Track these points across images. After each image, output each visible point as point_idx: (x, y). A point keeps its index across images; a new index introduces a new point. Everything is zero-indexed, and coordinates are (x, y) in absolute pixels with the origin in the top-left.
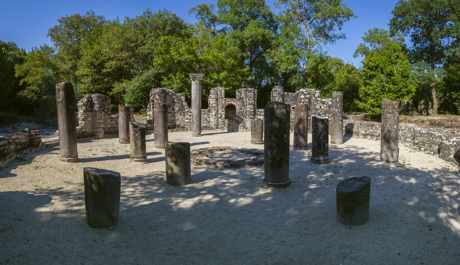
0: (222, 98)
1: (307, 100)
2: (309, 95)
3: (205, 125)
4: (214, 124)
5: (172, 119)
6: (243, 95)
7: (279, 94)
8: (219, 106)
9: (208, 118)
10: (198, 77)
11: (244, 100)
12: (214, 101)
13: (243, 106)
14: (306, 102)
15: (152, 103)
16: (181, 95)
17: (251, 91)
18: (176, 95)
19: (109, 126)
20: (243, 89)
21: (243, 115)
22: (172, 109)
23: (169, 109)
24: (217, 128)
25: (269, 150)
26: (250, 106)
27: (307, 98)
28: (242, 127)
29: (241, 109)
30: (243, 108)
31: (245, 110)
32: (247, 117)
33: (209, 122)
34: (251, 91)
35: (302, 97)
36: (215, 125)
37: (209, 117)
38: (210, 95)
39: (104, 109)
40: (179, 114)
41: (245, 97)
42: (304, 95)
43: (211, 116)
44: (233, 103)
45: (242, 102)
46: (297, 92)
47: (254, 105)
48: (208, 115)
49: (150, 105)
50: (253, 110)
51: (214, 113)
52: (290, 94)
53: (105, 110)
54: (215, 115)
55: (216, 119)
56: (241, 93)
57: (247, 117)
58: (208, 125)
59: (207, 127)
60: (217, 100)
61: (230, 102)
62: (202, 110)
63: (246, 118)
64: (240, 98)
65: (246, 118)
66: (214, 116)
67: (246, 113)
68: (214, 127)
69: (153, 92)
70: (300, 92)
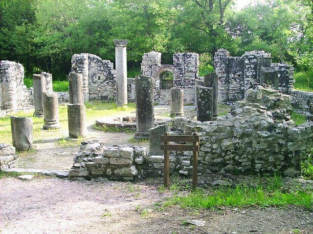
1: (252, 66)
2: (255, 60)
5: (99, 89)
6: (181, 60)
7: (221, 59)
8: (153, 74)
11: (182, 67)
13: (181, 74)
14: (251, 67)
16: (108, 62)
18: (102, 62)
19: (23, 98)
22: (98, 78)
23: (94, 77)
27: (252, 63)
29: (178, 77)
30: (182, 75)
31: (183, 78)
35: (247, 61)
40: (106, 84)
41: (183, 63)
42: (249, 59)
44: (169, 70)
45: (180, 69)
46: (243, 56)
52: (235, 58)
57: (186, 87)
60: (150, 67)
61: (166, 69)
64: (178, 64)
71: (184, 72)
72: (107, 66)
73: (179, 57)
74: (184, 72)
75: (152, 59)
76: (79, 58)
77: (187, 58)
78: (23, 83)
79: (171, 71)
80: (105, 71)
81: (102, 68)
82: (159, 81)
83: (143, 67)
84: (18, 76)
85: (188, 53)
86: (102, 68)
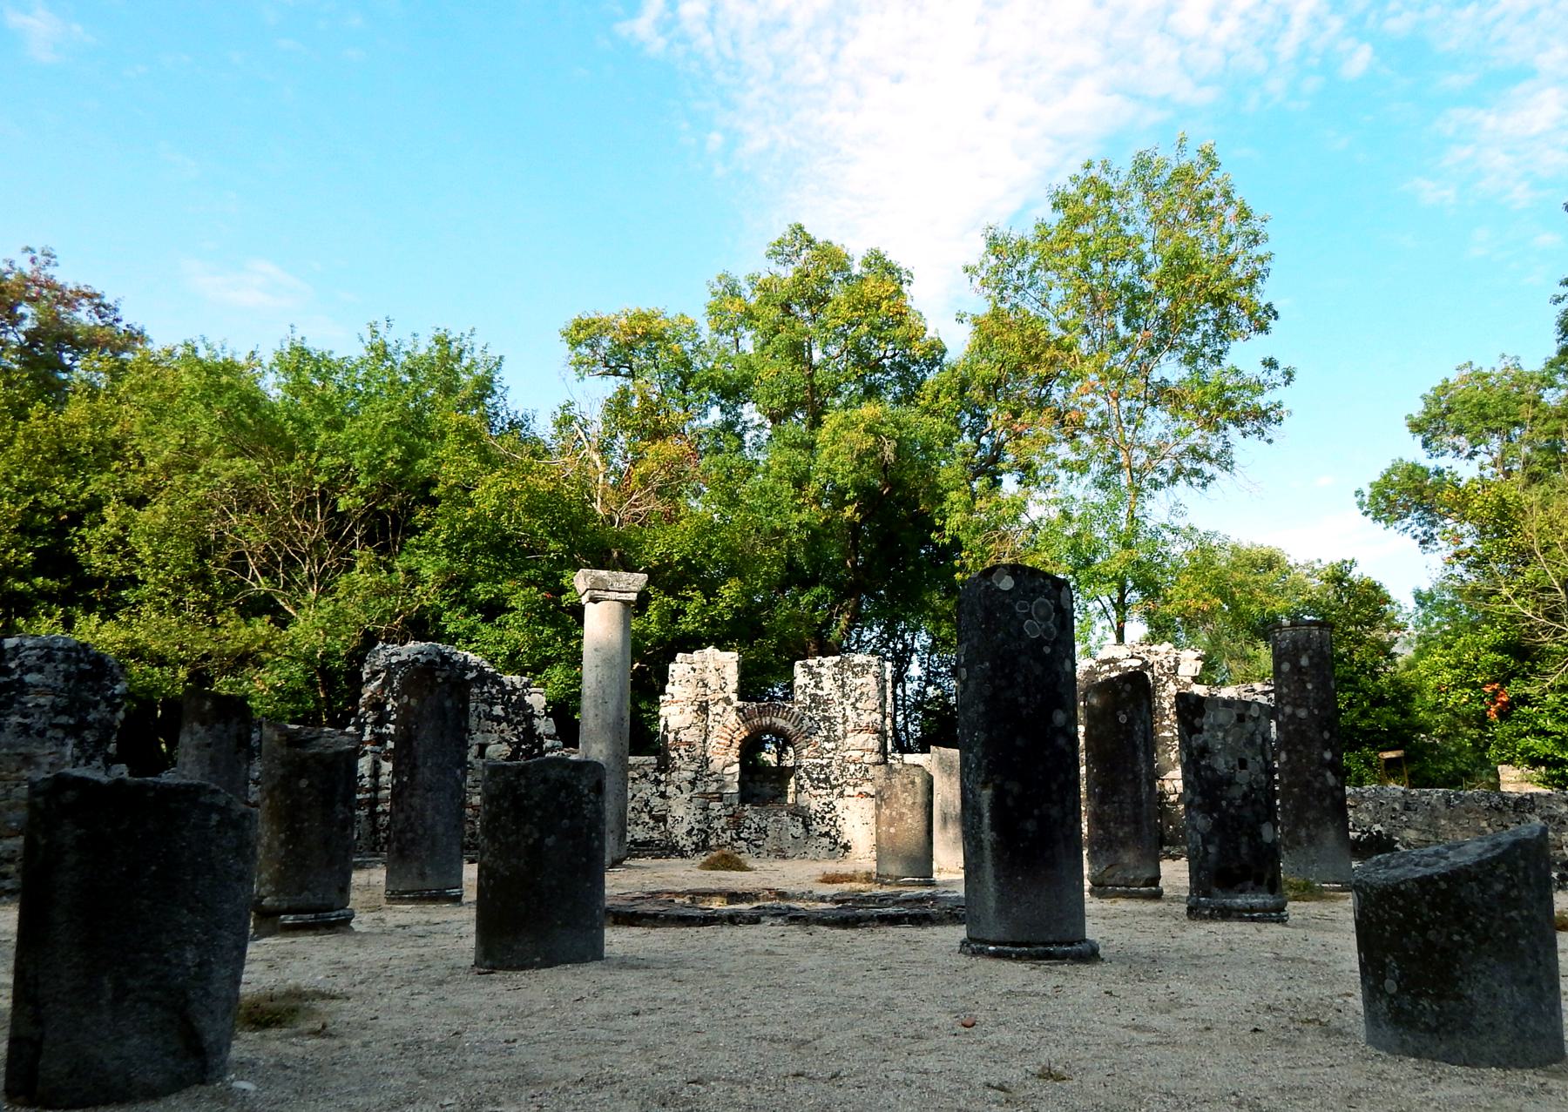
0: (728, 701)
3: (639, 834)
4: (685, 827)
6: (827, 684)
8: (712, 741)
9: (656, 802)
10: (616, 586)
11: (835, 711)
12: (689, 716)
15: (371, 716)
16: (527, 685)
17: (865, 668)
18: (502, 684)
20: (830, 660)
21: (827, 780)
24: (701, 847)
25: (985, 785)
26: (864, 736)
28: (826, 841)
30: (831, 745)
32: (849, 790)
33: (663, 819)
34: (865, 668)
36: (689, 833)
37: (663, 795)
38: (669, 688)
39: (83, 725)
41: (836, 695)
43: (671, 790)
47: (882, 733)
48: (658, 782)
49: (360, 727)
50: (875, 758)
51: (689, 775)
53: (89, 736)
54: (693, 783)
55: (698, 801)
56: (816, 676)
57: (849, 790)
58: (656, 835)
59: (647, 843)
60: (703, 709)
61: (766, 721)
62: (632, 760)
63: (841, 795)
64: (814, 698)
65: (841, 795)
66: (685, 785)
67: (843, 770)
68: (687, 843)
69: (381, 661)
70: (1105, 662)
71: (839, 733)
72: (521, 698)
73: (823, 670)
74: (840, 728)
75: (713, 680)
76: (404, 657)
77: (856, 675)
78: (112, 748)
79: (790, 727)
80: (510, 722)
81: (498, 710)
82: (736, 768)
83: (674, 709)
84: (92, 716)
85: (859, 658)
86: (498, 710)
